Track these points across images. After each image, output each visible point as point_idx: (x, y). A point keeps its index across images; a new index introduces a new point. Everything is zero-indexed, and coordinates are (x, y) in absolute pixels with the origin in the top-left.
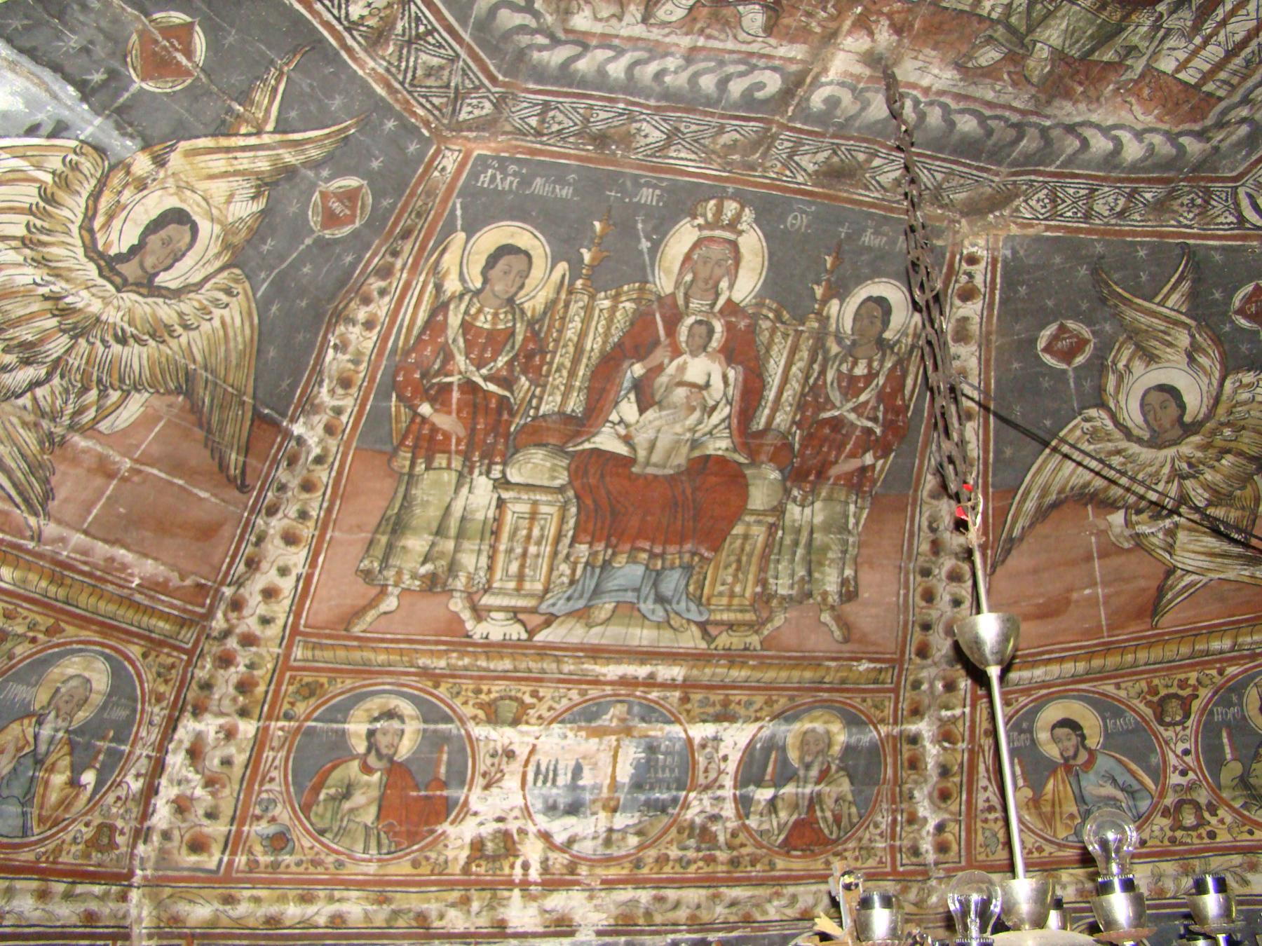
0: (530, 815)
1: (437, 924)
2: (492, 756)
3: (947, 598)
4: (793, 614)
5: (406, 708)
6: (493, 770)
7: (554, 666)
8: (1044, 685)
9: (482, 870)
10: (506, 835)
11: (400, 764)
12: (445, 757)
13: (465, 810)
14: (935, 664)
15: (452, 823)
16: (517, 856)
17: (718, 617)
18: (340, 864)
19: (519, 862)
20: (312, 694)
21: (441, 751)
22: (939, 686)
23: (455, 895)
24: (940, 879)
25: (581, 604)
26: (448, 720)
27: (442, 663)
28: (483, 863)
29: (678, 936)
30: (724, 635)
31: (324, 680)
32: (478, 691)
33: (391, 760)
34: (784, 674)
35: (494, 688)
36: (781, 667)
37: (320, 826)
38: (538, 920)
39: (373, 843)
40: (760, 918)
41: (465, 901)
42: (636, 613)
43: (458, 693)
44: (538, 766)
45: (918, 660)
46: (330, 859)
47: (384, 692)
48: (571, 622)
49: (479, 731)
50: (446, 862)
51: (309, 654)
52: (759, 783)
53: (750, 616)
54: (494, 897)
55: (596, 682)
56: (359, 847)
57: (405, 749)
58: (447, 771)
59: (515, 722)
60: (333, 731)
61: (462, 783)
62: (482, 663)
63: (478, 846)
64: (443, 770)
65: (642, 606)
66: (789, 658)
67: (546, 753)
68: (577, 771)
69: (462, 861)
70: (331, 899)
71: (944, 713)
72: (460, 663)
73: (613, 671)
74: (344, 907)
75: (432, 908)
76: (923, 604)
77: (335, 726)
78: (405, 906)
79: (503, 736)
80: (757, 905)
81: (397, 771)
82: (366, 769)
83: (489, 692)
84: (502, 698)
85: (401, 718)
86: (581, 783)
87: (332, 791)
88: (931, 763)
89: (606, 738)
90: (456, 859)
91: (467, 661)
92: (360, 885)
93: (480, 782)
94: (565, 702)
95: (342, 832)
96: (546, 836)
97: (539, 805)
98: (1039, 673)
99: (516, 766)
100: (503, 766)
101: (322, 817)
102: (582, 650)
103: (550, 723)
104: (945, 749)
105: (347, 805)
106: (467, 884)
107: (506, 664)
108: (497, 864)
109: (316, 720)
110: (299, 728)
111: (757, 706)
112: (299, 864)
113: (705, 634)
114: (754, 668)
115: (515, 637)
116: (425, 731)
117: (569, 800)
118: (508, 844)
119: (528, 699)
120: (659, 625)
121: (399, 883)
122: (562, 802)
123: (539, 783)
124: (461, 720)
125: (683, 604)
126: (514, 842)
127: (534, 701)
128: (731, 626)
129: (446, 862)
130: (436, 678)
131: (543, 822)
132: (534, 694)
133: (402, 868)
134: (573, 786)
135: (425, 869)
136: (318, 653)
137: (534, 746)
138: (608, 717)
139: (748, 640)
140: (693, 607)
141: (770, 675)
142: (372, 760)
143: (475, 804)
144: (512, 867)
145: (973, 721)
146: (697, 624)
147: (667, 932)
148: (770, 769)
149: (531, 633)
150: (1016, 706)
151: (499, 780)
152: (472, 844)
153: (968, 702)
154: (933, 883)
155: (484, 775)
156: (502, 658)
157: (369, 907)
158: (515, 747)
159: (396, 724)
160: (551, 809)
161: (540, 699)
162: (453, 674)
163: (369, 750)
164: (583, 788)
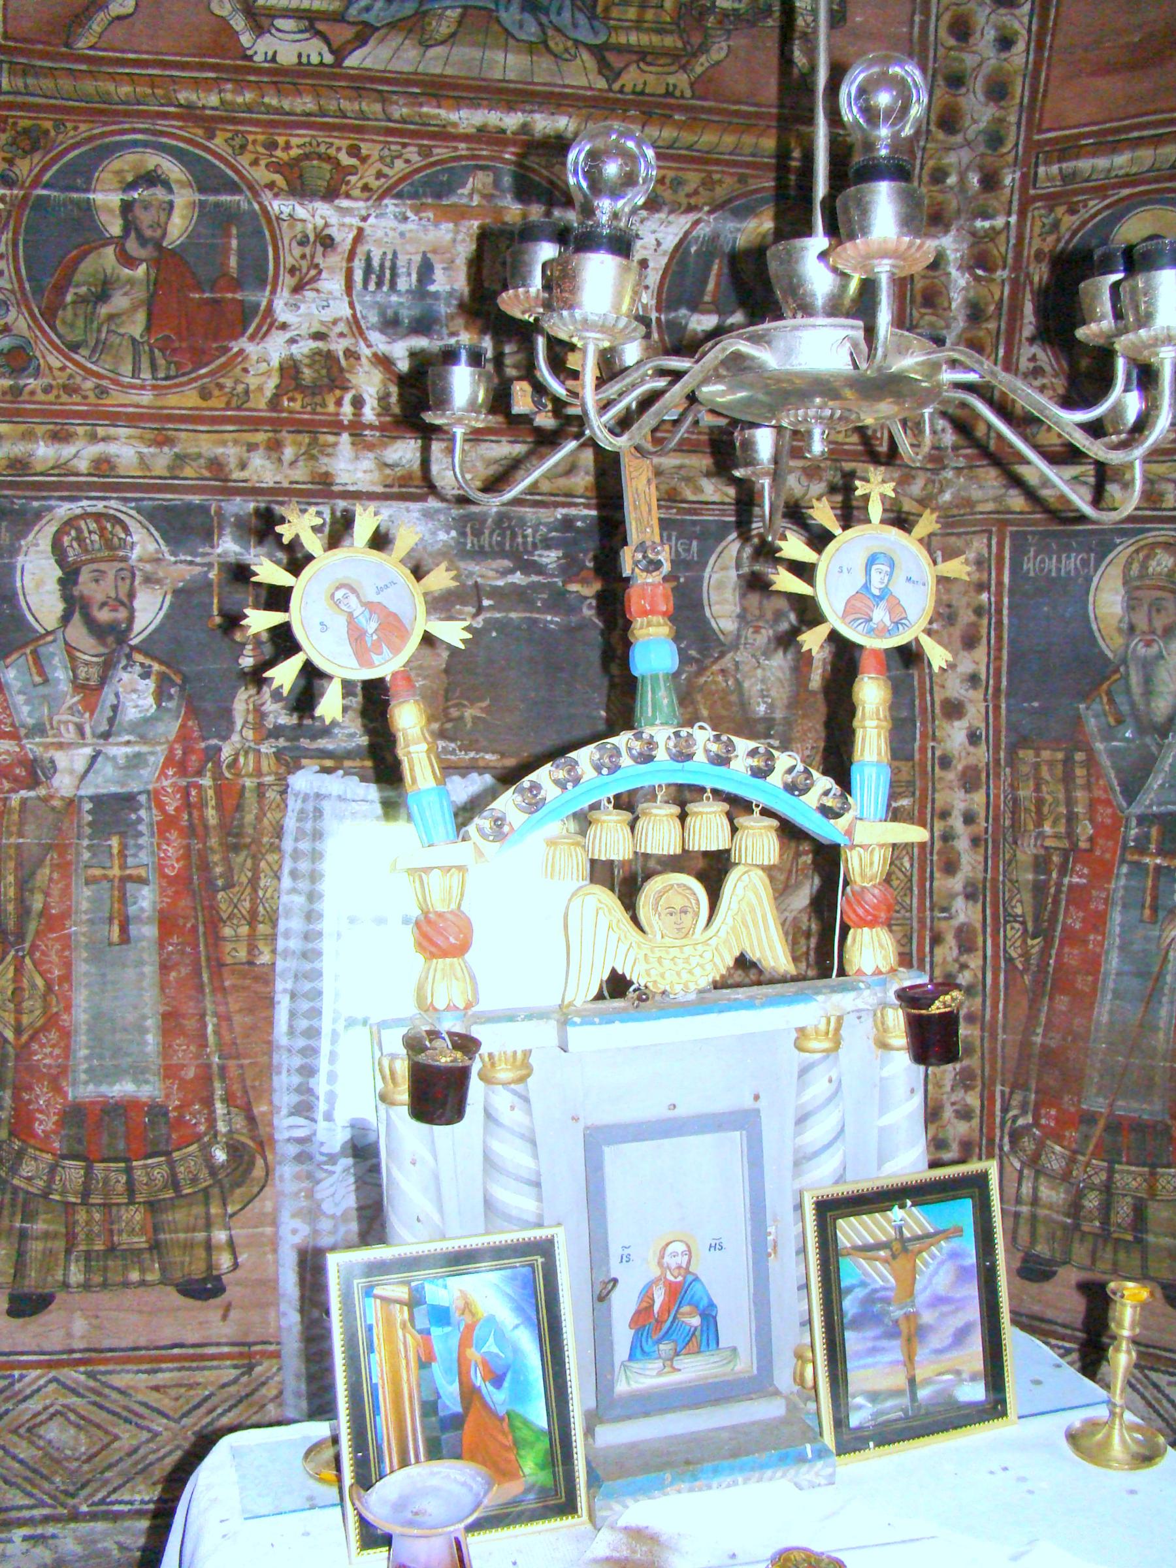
0: (362, 333)
1: (236, 475)
2: (301, 244)
3: (991, 34)
4: (740, 41)
5: (173, 170)
6: (304, 264)
7: (377, 107)
8: (1129, 180)
9: (296, 406)
10: (329, 356)
11: (173, 253)
12: (234, 243)
13: (269, 323)
14: (968, 144)
15: (252, 338)
16: (346, 389)
17: (623, 40)
18: (102, 392)
19: (348, 398)
20: (34, 149)
21: (229, 236)
22: (974, 180)
23: (260, 437)
24: (958, 470)
25: (409, 8)
26: (234, 188)
27: (213, 100)
28: (299, 397)
29: (573, 511)
30: (633, 68)
31: (48, 125)
32: (272, 146)
33: (158, 246)
34: (729, 140)
35: (295, 141)
36: (726, 127)
37: (72, 337)
38: (376, 476)
39: (145, 364)
40: (692, 498)
41: (275, 447)
42: (495, 27)
43: (243, 147)
44: (368, 260)
45: (940, 135)
46: (89, 384)
47: (135, 144)
48: (395, 40)
49: (280, 206)
50: (247, 392)
51: (20, 83)
52: (695, 306)
53: (670, 41)
54: (314, 442)
55: (445, 135)
56: (127, 368)
57: (178, 227)
58: (239, 265)
59: (331, 194)
60: (72, 201)
61: (262, 283)
62: (272, 100)
63: (290, 370)
64: (233, 262)
65: (504, 16)
66: (737, 113)
67: (378, 242)
68: (426, 270)
69: (269, 393)
70: (93, 438)
71: (979, 224)
72: (240, 100)
73: (467, 119)
74: (112, 449)
75: (231, 453)
76: (952, 42)
77: (75, 195)
78: (193, 450)
79: (316, 214)
80: (688, 480)
81: (168, 262)
82: (128, 261)
83: (288, 147)
84: (307, 156)
85: (167, 185)
86: (432, 288)
87: (83, 290)
88: (957, 300)
89: (467, 223)
90: (260, 389)
91: (249, 96)
92: (132, 420)
93: (287, 281)
94: (399, 164)
95: (100, 348)
96: (384, 362)
97: (374, 319)
98: (1121, 160)
99: (335, 261)
100: (318, 259)
101: (72, 326)
102: (416, 84)
103: (381, 198)
104: (977, 279)
105: (104, 310)
106: (275, 425)
107: (306, 103)
108: (318, 399)
109: (45, 187)
110: (25, 198)
111: (689, 189)
112: (47, 390)
113: (604, 66)
114: (680, 126)
115: (315, 60)
116: (202, 204)
117: (416, 312)
118: (330, 374)
119: (346, 160)
120: (531, 48)
121: (183, 419)
122: (406, 315)
123: (372, 287)
124: (251, 188)
125: (567, 15)
126: (341, 370)
127: (353, 161)
128: (643, 55)
129: (247, 392)
130: (209, 123)
131: (380, 342)
132: (354, 151)
133: (186, 399)
134: (421, 292)
135: (217, 402)
136: (30, 81)
137: (360, 230)
138: (465, 191)
139: (671, 80)
140: (582, 20)
141: (707, 139)
142: (132, 246)
143: (282, 313)
144: (339, 403)
145: (1020, 238)
146: (590, 48)
147: (556, 505)
148: (711, 286)
149: (339, 54)
150: (1084, 214)
151: (315, 279)
152: (281, 368)
153: (1015, 207)
154: (949, 474)
155: (292, 271)
156: (299, 93)
157: (145, 450)
158: (333, 231)
159: (159, 193)
160: (391, 324)
161: (363, 160)
162: (228, 117)
163: (126, 230)
164: (436, 296)
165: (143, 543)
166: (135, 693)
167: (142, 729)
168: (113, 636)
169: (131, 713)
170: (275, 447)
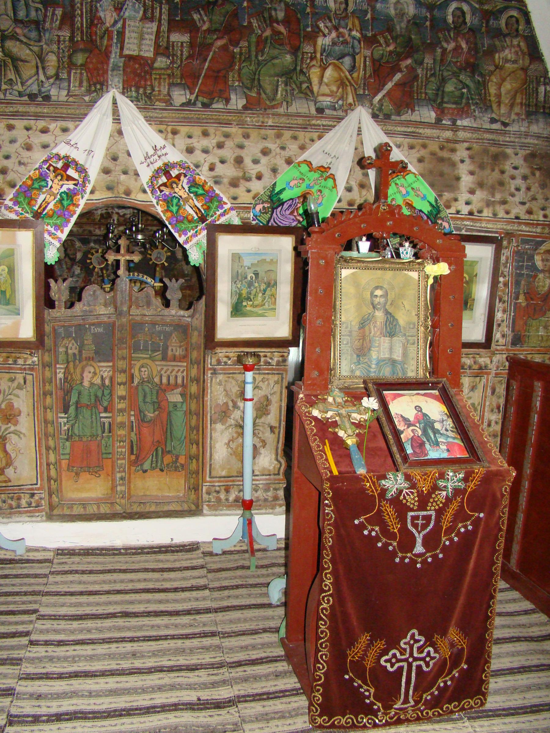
10: (108, 213)
41: (100, 228)
63: (102, 215)
75: (92, 229)
96: (118, 213)
131: (117, 210)
165: (78, 244)
166: (77, 270)
167: (78, 276)
168: (73, 260)
169: (76, 273)
170: (100, 228)
